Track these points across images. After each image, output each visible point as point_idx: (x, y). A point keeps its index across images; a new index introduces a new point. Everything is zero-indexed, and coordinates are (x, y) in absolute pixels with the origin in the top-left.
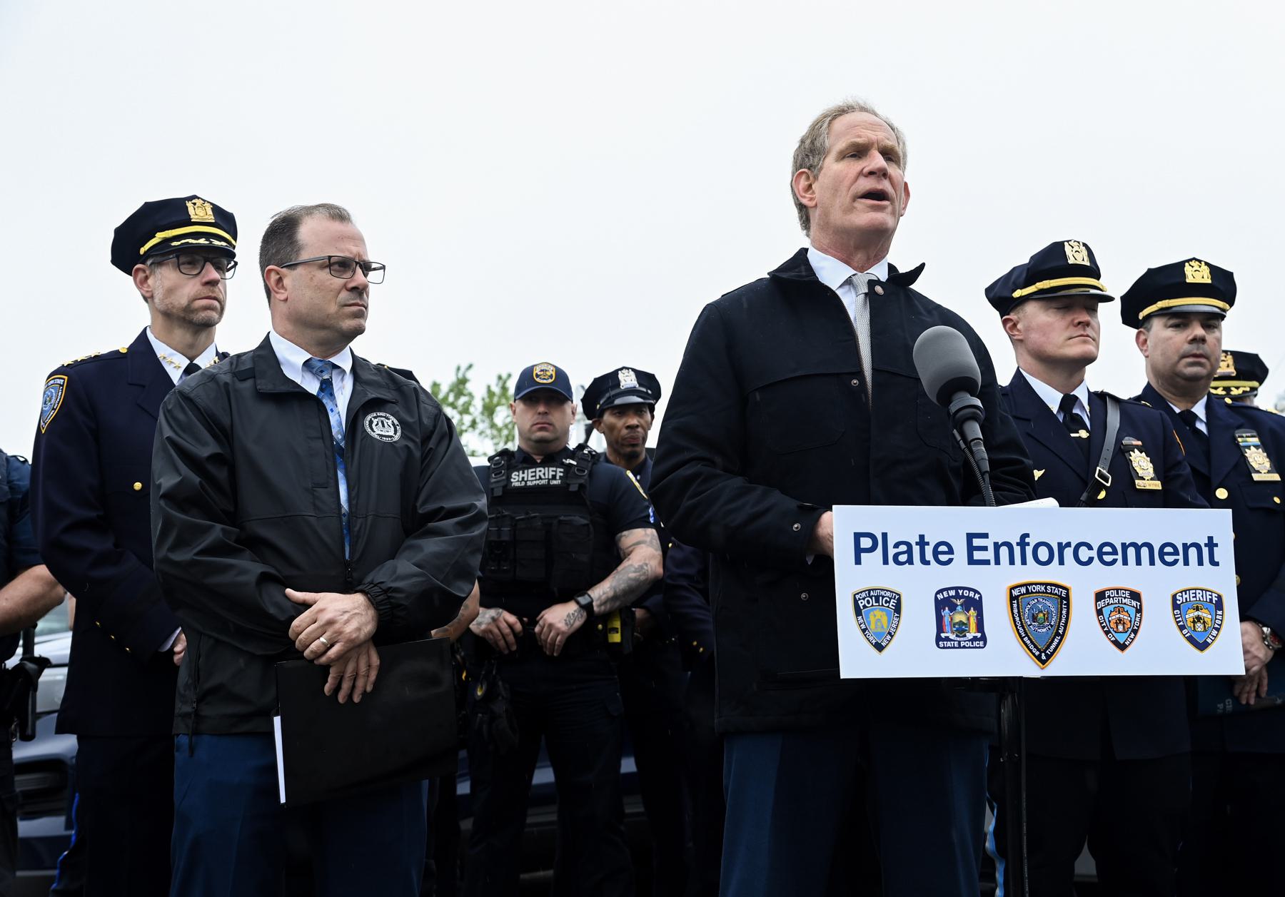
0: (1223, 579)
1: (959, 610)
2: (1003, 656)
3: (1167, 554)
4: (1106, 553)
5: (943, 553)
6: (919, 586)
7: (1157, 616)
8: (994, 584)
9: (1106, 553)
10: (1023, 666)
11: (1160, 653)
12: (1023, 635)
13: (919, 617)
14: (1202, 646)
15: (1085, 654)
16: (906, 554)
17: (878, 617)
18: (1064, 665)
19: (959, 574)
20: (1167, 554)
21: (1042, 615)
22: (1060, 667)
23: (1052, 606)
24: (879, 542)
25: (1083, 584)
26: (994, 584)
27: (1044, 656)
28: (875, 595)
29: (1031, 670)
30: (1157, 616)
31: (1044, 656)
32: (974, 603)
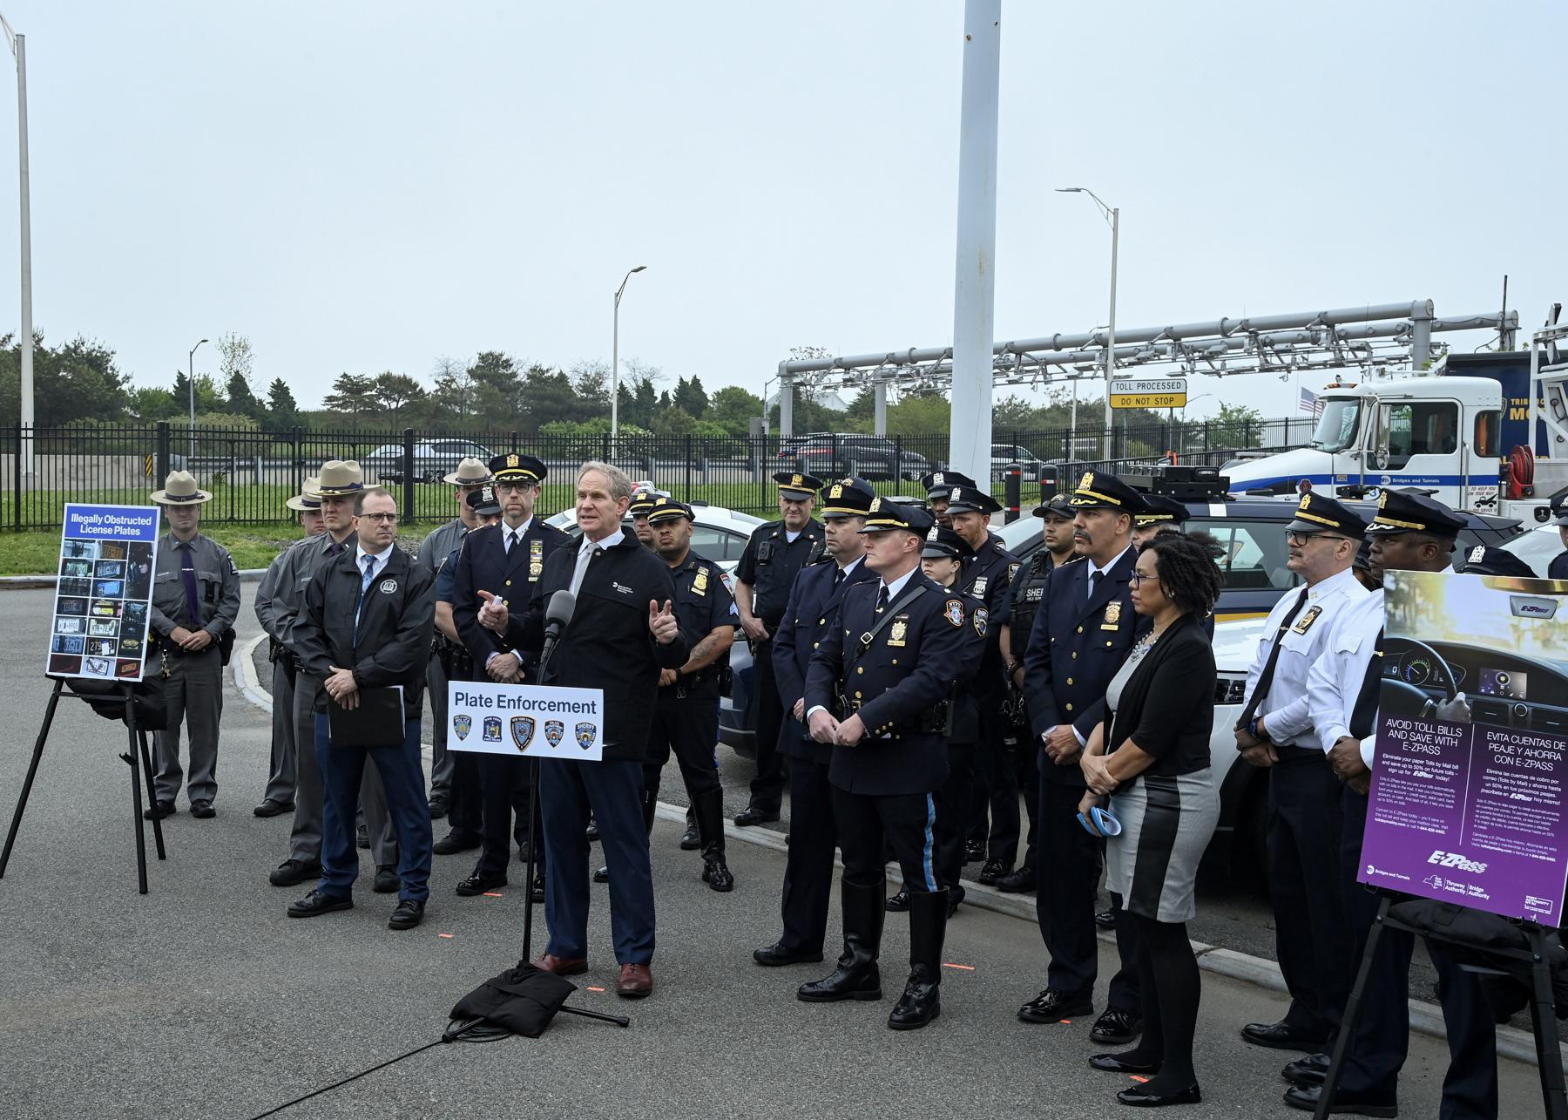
0: (597, 720)
1: (492, 725)
2: (506, 746)
3: (575, 708)
4: (552, 706)
5: (488, 702)
6: (478, 715)
7: (569, 735)
8: (506, 716)
9: (552, 706)
10: (515, 751)
11: (569, 749)
12: (515, 738)
13: (477, 728)
14: (585, 747)
15: (539, 747)
16: (476, 702)
17: (462, 726)
18: (530, 751)
19: (494, 711)
20: (575, 708)
21: (523, 730)
22: (528, 752)
23: (527, 726)
24: (465, 696)
25: (540, 717)
26: (506, 716)
27: (522, 747)
28: (462, 717)
29: (518, 752)
30: (569, 735)
31: (522, 747)
32: (499, 724)
